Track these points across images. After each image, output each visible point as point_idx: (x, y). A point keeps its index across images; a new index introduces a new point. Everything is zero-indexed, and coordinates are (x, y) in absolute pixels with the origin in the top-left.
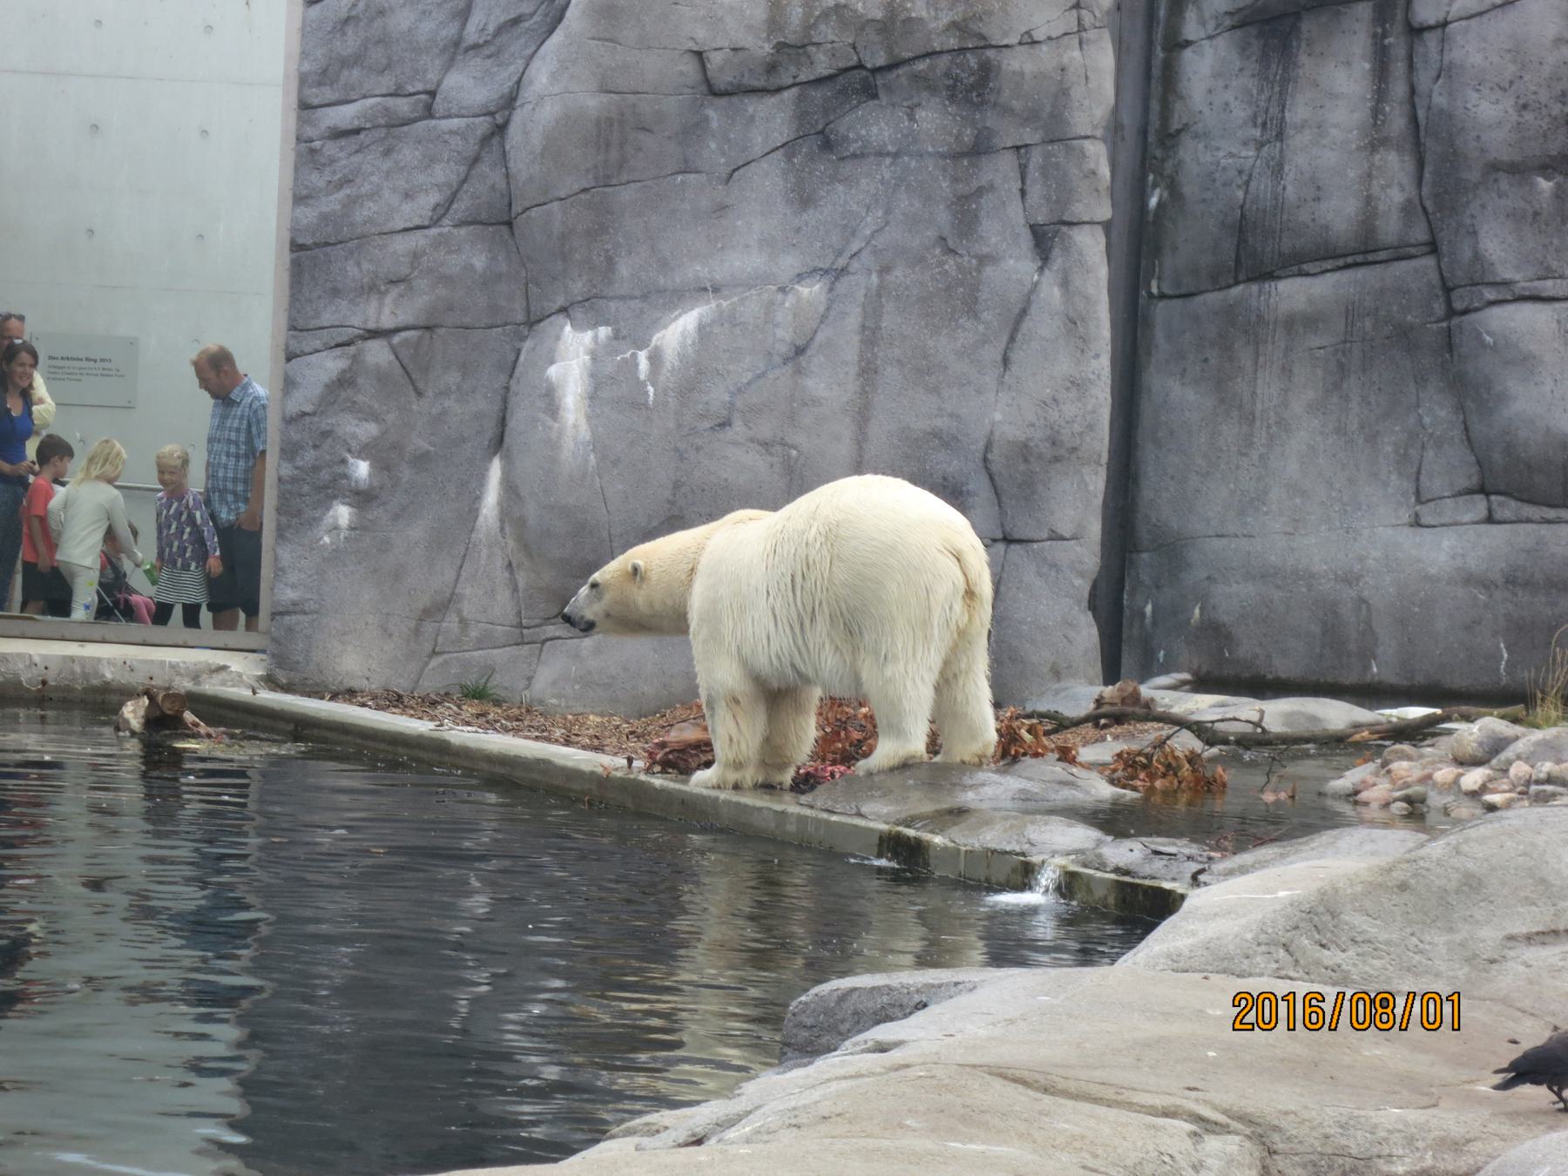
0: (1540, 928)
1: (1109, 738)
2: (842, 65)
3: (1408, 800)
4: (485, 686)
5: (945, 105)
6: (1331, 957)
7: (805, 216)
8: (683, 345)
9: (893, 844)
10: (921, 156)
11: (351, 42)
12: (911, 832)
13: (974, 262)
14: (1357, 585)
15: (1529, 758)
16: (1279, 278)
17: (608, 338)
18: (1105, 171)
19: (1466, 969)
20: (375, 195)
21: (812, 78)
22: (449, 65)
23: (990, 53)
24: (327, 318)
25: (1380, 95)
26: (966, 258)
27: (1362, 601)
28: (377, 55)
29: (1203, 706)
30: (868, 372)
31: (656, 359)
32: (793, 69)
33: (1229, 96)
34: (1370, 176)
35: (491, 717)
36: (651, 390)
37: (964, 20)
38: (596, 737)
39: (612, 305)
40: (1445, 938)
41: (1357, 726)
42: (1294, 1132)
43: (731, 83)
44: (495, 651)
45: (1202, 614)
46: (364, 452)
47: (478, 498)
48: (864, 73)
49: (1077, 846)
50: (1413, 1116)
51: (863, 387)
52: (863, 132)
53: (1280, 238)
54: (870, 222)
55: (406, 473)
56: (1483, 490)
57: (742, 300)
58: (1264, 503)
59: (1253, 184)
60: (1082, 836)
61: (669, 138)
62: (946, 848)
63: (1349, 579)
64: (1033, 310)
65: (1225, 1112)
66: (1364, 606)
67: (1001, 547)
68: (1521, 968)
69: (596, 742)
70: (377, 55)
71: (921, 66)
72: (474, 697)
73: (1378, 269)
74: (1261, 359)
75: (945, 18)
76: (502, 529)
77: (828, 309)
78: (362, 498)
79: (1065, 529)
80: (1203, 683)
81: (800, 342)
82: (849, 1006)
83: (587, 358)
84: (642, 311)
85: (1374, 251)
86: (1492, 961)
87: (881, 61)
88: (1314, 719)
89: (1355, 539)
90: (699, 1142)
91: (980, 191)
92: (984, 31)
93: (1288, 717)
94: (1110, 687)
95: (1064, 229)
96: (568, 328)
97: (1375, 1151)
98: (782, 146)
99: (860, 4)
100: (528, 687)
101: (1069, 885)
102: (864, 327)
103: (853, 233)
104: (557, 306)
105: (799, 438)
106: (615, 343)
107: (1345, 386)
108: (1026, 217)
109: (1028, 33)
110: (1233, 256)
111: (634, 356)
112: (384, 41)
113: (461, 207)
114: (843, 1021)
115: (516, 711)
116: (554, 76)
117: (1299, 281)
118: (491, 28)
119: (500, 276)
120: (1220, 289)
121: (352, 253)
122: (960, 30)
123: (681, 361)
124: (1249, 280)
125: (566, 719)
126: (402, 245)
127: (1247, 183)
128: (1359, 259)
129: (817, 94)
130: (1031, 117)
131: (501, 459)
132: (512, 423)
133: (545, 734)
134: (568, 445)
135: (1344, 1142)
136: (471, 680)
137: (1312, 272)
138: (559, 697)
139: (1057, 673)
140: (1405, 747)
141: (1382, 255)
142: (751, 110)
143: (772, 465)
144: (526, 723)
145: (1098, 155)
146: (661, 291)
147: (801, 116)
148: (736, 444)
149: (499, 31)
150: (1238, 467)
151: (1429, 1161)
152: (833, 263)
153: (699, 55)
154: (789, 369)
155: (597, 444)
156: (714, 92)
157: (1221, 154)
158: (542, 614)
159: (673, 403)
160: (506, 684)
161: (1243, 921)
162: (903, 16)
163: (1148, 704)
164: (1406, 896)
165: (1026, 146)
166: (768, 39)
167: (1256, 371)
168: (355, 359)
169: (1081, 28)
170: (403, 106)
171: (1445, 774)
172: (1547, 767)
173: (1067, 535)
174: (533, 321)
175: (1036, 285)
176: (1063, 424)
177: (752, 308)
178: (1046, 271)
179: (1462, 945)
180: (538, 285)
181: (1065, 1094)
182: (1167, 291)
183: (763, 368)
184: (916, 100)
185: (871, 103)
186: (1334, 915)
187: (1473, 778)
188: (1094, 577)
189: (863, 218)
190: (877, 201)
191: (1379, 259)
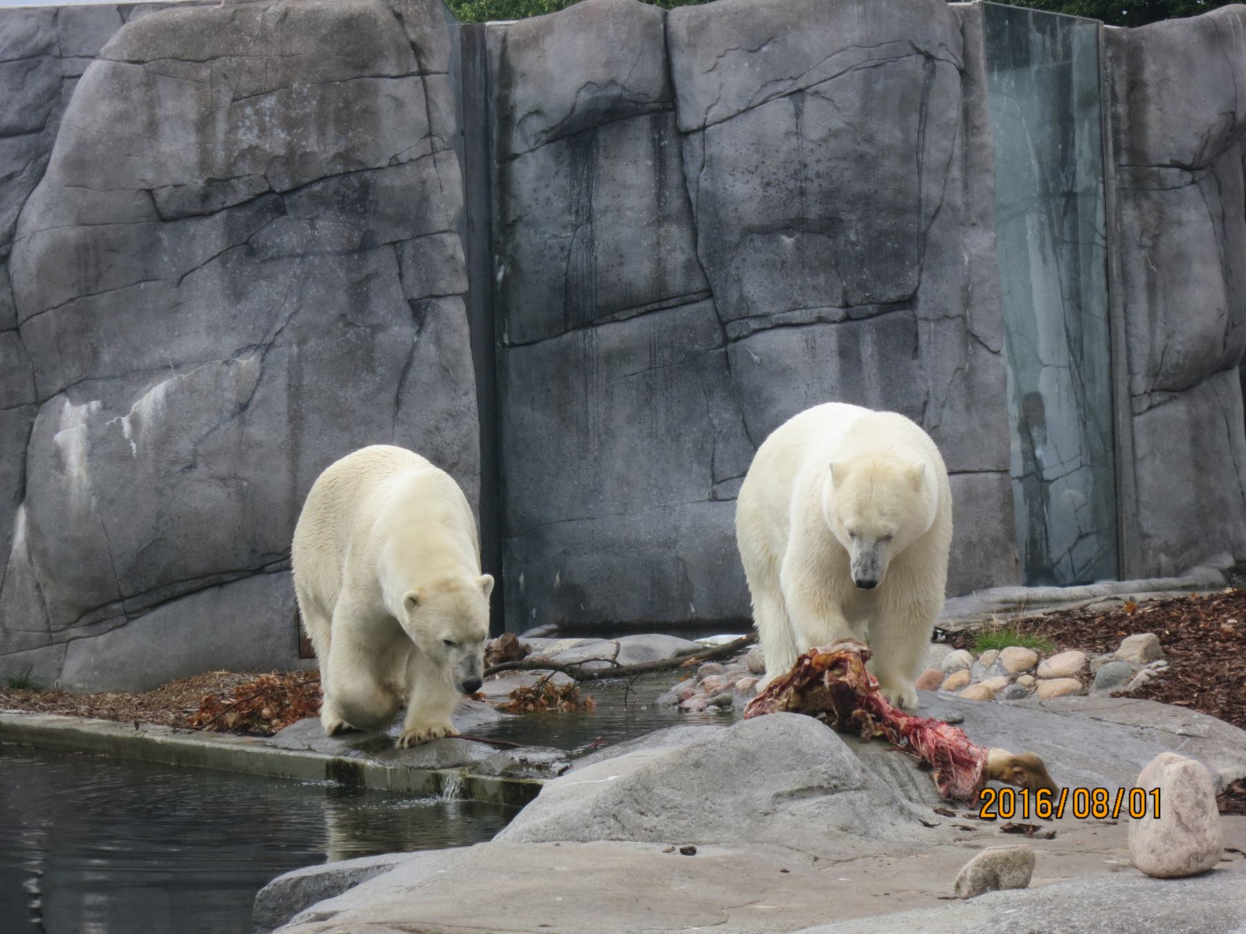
2: (257, 191)
3: (719, 703)
4: (27, 679)
5: (337, 216)
6: (648, 821)
7: (239, 306)
8: (155, 410)
10: (323, 255)
14: (675, 548)
16: (598, 325)
17: (98, 408)
18: (461, 255)
19: (748, 821)
21: (236, 202)
23: (368, 174)
25: (661, 184)
26: (362, 328)
27: (679, 559)
29: (567, 649)
30: (296, 419)
32: (221, 197)
33: (548, 193)
34: (658, 244)
35: (33, 701)
36: (134, 445)
37: (347, 151)
38: (113, 709)
40: (732, 799)
41: (681, 654)
43: (175, 211)
44: (32, 652)
45: (561, 578)
47: (9, 538)
48: (275, 196)
51: (293, 430)
52: (278, 240)
53: (596, 296)
57: (197, 373)
58: (600, 493)
59: (573, 256)
61: (133, 256)
62: (376, 769)
63: (668, 544)
64: (416, 363)
66: (681, 564)
68: (788, 817)
69: (113, 713)
71: (317, 188)
72: (19, 687)
73: (670, 313)
74: (590, 386)
75: (332, 151)
76: (30, 559)
77: (262, 374)
80: (565, 631)
81: (243, 401)
83: (84, 425)
84: (122, 388)
86: (766, 814)
87: (287, 185)
88: (648, 650)
89: (670, 514)
91: (369, 278)
92: (361, 158)
93: (631, 652)
94: (496, 639)
95: (434, 301)
96: (68, 404)
98: (218, 256)
99: (267, 146)
100: (58, 677)
101: (467, 789)
102: (289, 386)
103: (276, 316)
104: (58, 388)
105: (249, 473)
106: (103, 412)
107: (653, 401)
108: (404, 293)
109: (395, 157)
110: (562, 311)
111: (119, 421)
114: (297, 902)
115: (51, 695)
116: (42, 215)
117: (613, 325)
119: (13, 368)
120: (555, 336)
122: (344, 158)
123: (155, 422)
124: (575, 328)
125: (89, 698)
127: (568, 257)
128: (656, 306)
129: (241, 215)
130: (401, 219)
131: (25, 506)
133: (74, 710)
134: (74, 490)
136: (16, 674)
137: (621, 319)
138: (84, 681)
140: (714, 665)
141: (672, 302)
142: (192, 230)
143: (229, 495)
144: (59, 703)
145: (454, 244)
146: (136, 371)
147: (230, 231)
148: (201, 481)
150: (579, 467)
152: (263, 340)
154: (236, 421)
155: (98, 489)
156: (163, 219)
157: (547, 236)
158: (65, 620)
159: (151, 454)
160: (42, 676)
161: (582, 801)
162: (301, 151)
163: (525, 651)
164: (700, 771)
165: (401, 241)
166: (200, 176)
167: (586, 396)
169: (434, 151)
174: (40, 402)
175: (417, 343)
179: (744, 803)
180: (42, 373)
182: (515, 341)
183: (217, 422)
184: (315, 214)
185: (282, 218)
189: (282, 305)
190: (292, 291)
191: (671, 305)
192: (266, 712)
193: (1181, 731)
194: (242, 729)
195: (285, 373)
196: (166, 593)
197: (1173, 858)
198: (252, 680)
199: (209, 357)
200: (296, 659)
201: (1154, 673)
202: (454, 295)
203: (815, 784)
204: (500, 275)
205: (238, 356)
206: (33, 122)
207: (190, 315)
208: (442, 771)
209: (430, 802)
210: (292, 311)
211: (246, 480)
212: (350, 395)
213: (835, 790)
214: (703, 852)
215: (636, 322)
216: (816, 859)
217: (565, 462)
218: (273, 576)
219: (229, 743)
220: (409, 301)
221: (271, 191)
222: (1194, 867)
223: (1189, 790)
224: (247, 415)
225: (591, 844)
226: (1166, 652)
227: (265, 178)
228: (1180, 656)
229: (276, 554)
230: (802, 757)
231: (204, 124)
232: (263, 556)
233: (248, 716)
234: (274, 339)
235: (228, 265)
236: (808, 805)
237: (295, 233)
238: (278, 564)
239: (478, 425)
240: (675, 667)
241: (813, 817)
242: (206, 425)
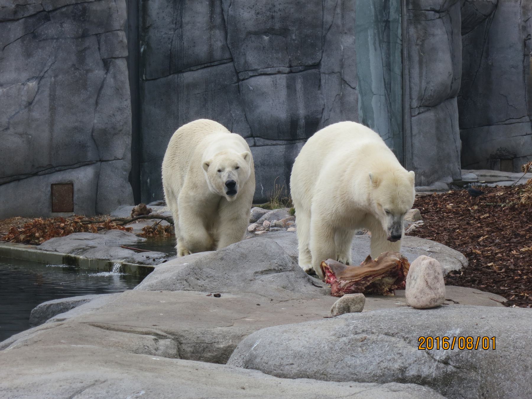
0: (266, 269)
1: (137, 222)
2: (38, 10)
6: (200, 282)
7: (29, 60)
10: (66, 39)
12: (73, 255)
13: (85, 72)
15: (269, 219)
16: (184, 72)
18: (125, 40)
21: (29, 15)
23: (86, 5)
25: (212, 12)
26: (82, 71)
30: (53, 109)
34: (210, 38)
42: (187, 337)
48: (45, 13)
49: (126, 256)
50: (225, 329)
52: (46, 32)
56: (252, 136)
57: (10, 88)
59: (173, 42)
60: (127, 253)
62: (84, 260)
65: (165, 332)
67: (99, 163)
68: (260, 282)
71: (64, 10)
73: (215, 68)
74: (180, 98)
77: (38, 90)
85: (213, 62)
86: (251, 280)
87: (51, 8)
91: (85, 49)
94: (137, 206)
95: (113, 60)
97: (213, 341)
98: (20, 38)
101: (123, 268)
102: (50, 95)
103: (45, 65)
107: (207, 105)
114: (49, 315)
117: (190, 73)
120: (165, 77)
124: (174, 73)
127: (172, 42)
128: (209, 64)
129: (31, 20)
135: (203, 339)
139: (120, 203)
141: (216, 63)
142: (9, 27)
143: (23, 141)
145: (122, 35)
154: (27, 110)
157: (163, 33)
161: (172, 273)
163: (149, 211)
164: (223, 262)
165: (99, 33)
166: (13, 3)
172: (275, 222)
173: (120, 158)
176: (117, 123)
178: (108, 74)
179: (241, 276)
181: (114, 330)
182: (148, 78)
185: (48, 22)
186: (201, 269)
188: (130, 171)
192: (37, 234)
193: (428, 250)
194: (27, 242)
195: (48, 89)
197: (424, 300)
198: (31, 221)
199: (15, 81)
200: (50, 212)
201: (417, 226)
203: (272, 268)
204: (142, 50)
205: (28, 81)
207: (8, 63)
208: (112, 261)
209: (106, 274)
210: (52, 63)
211: (31, 135)
213: (280, 271)
214: (224, 296)
215: (200, 71)
216: (272, 300)
217: (168, 131)
218: (41, 177)
219: (21, 247)
220: (103, 60)
221: (44, 11)
222: (433, 304)
223: (432, 272)
224: (31, 107)
225: (176, 292)
226: (423, 217)
227: (41, 4)
228: (429, 219)
229: (43, 167)
230: (266, 256)
232: (37, 168)
233: (30, 236)
234: (44, 75)
235: (25, 42)
236: (269, 277)
237: (53, 29)
238: (44, 172)
239: (131, 114)
241: (271, 282)
242: (14, 111)
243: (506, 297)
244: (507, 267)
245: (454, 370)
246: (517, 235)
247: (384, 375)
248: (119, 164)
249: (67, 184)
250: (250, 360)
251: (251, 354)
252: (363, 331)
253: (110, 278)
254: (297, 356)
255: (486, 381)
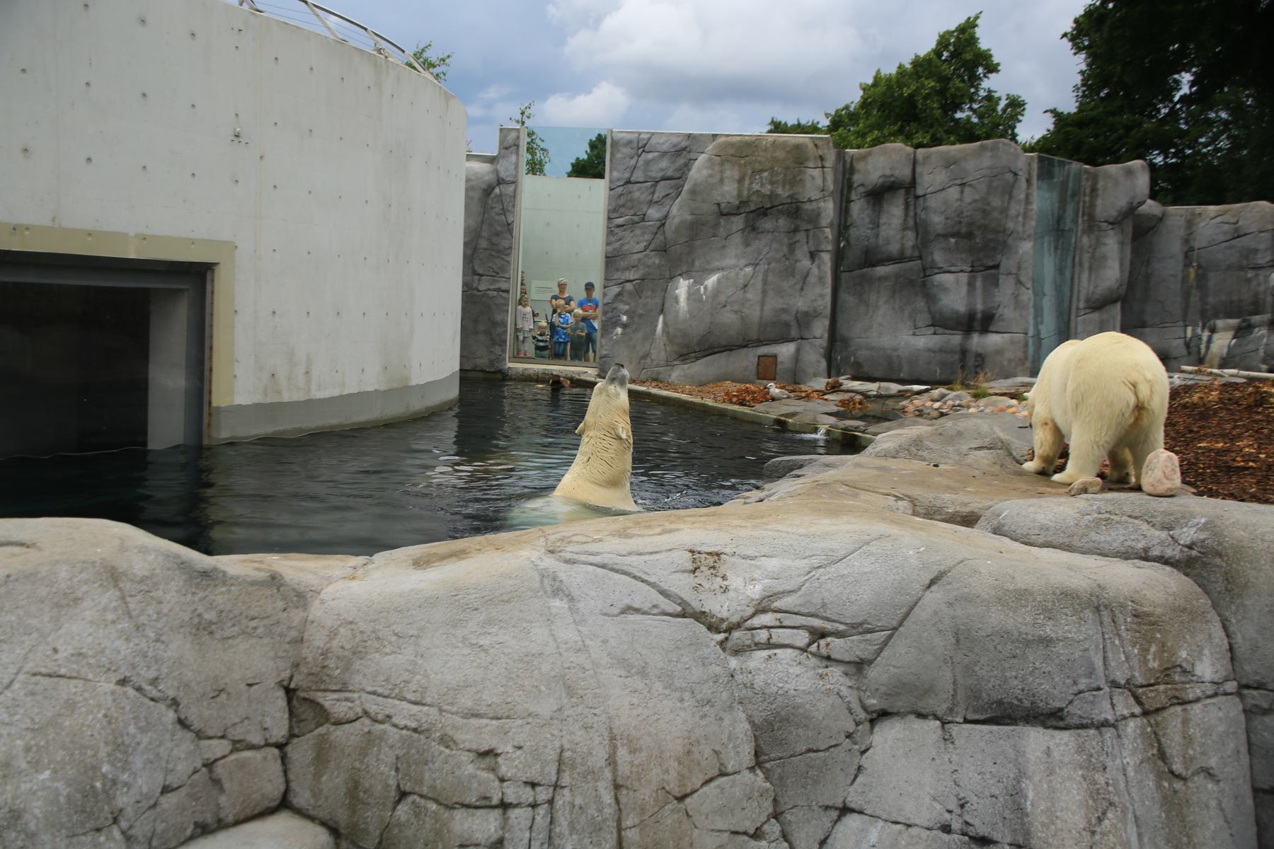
2: (758, 207)
9: (778, 422)
11: (622, 201)
12: (783, 418)
15: (952, 399)
18: (830, 236)
20: (628, 243)
22: (649, 207)
24: (615, 277)
25: (906, 215)
27: (899, 356)
28: (629, 204)
29: (857, 385)
30: (764, 292)
31: (705, 288)
33: (863, 215)
39: (694, 273)
41: (900, 391)
46: (625, 314)
47: (656, 326)
50: (954, 496)
54: (765, 250)
55: (636, 319)
56: (933, 325)
60: (832, 420)
63: (895, 350)
68: (973, 457)
70: (629, 204)
71: (780, 207)
75: (787, 194)
78: (624, 326)
79: (818, 335)
80: (854, 378)
82: (781, 466)
87: (769, 206)
88: (888, 389)
90: (762, 501)
91: (796, 242)
101: (828, 433)
105: (745, 310)
112: (631, 200)
113: (652, 246)
116: (678, 210)
118: (661, 196)
121: (622, 259)
126: (636, 257)
129: (751, 215)
130: (810, 221)
132: (666, 306)
136: (654, 376)
139: (815, 375)
145: (828, 232)
146: (707, 270)
147: (747, 221)
149: (663, 197)
151: (957, 509)
153: (718, 204)
155: (690, 312)
156: (722, 214)
159: (710, 300)
163: (841, 385)
168: (623, 287)
170: (636, 218)
171: (929, 404)
172: (957, 402)
177: (732, 275)
179: (957, 450)
187: (937, 405)
194: (742, 404)
196: (711, 351)
197: (1161, 489)
198: (743, 386)
199: (735, 266)
202: (827, 251)
204: (842, 245)
206: (677, 175)
212: (785, 285)
213: (991, 448)
214: (941, 467)
215: (892, 266)
221: (763, 207)
222: (1169, 493)
223: (1169, 464)
231: (741, 181)
240: (901, 395)
241: (983, 458)
243: (1195, 488)
244: (1189, 460)
245: (1199, 555)
246: (1191, 431)
247: (1127, 552)
248: (818, 342)
249: (771, 356)
250: (998, 527)
251: (999, 523)
252: (1107, 512)
253: (816, 441)
254: (1044, 528)
255: (1231, 568)
